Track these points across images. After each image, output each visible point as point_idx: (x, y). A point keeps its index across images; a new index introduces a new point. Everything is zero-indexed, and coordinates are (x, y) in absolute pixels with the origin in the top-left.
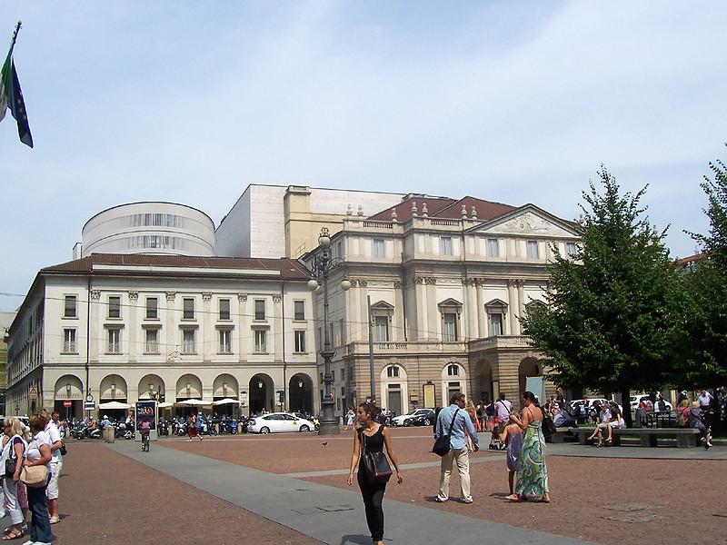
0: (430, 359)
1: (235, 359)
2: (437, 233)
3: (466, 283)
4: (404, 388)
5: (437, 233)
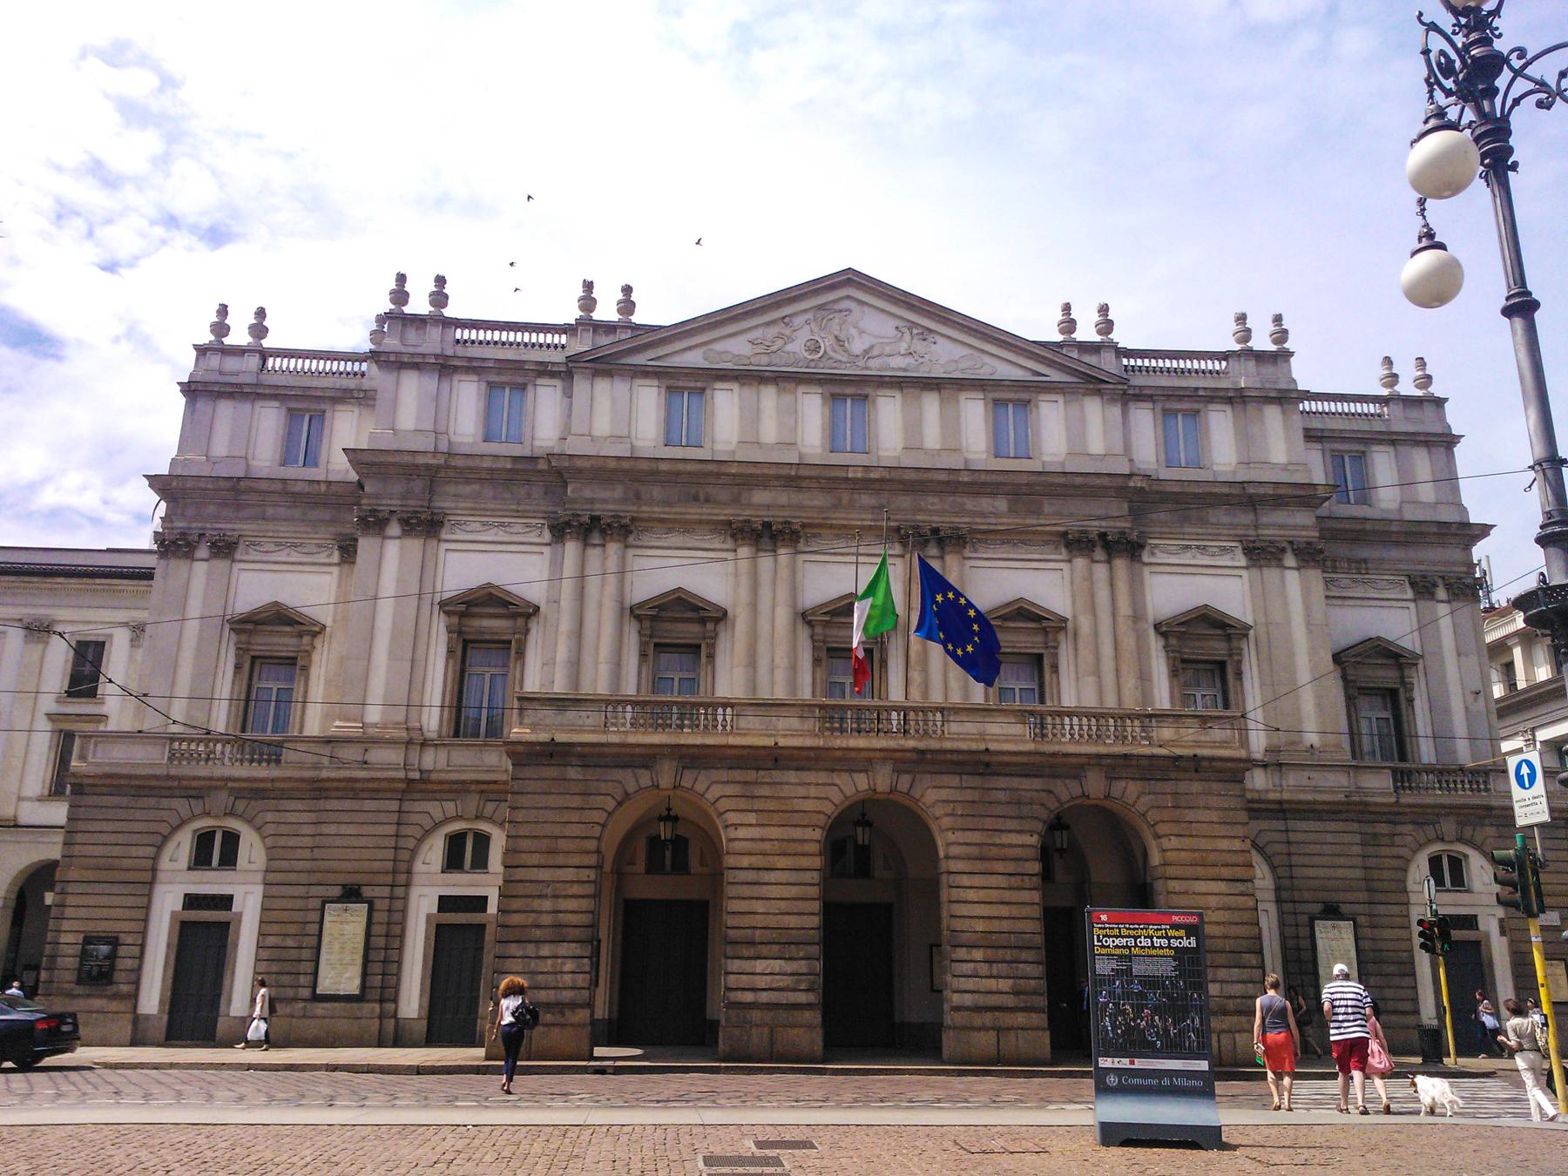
2: (474, 367)
5: (474, 367)
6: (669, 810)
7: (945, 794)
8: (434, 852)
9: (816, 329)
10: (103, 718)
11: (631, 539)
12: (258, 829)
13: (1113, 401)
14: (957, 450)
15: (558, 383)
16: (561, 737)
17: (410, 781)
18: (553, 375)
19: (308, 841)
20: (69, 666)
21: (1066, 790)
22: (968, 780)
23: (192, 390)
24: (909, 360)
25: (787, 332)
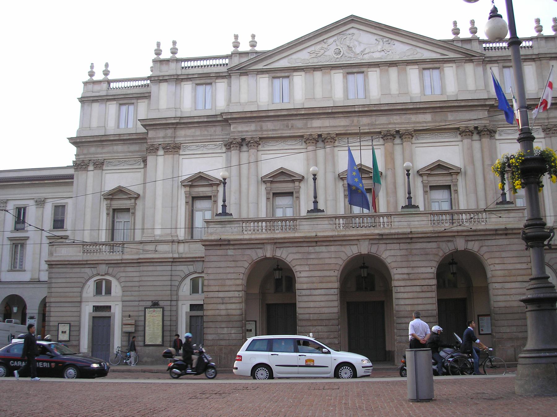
0: (159, 268)
1: (26, 277)
2: (188, 78)
3: (229, 146)
4: (117, 311)
6: (278, 266)
7: (392, 253)
8: (186, 287)
10: (66, 237)
11: (260, 147)
12: (118, 279)
13: (478, 65)
14: (407, 93)
15: (226, 81)
16: (223, 237)
17: (174, 258)
18: (223, 77)
19: (137, 284)
20: (53, 216)
21: (447, 248)
22: (403, 246)
23: (83, 100)
24: (383, 53)
25: (325, 46)
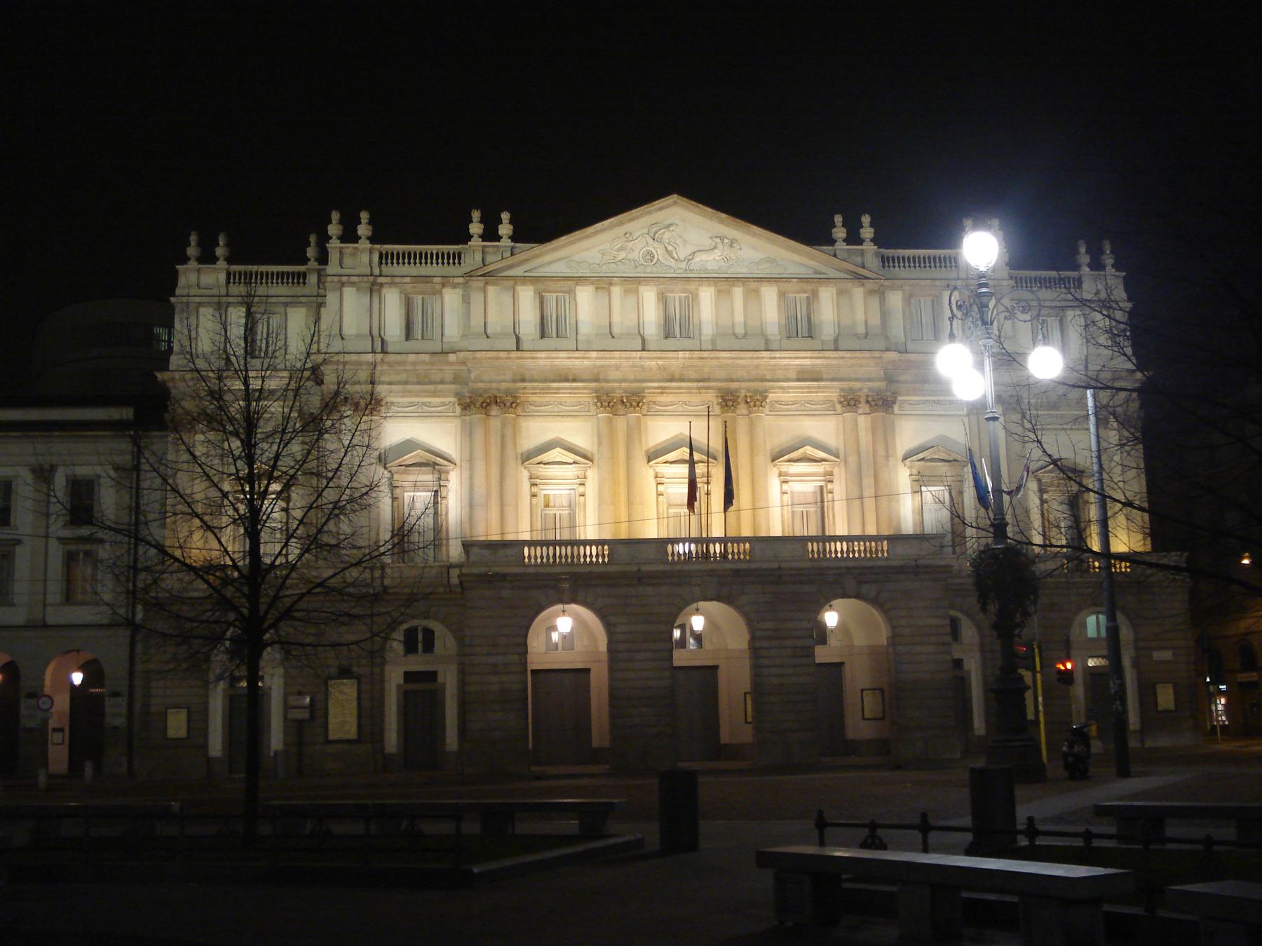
9: (651, 241)
13: (872, 292)
